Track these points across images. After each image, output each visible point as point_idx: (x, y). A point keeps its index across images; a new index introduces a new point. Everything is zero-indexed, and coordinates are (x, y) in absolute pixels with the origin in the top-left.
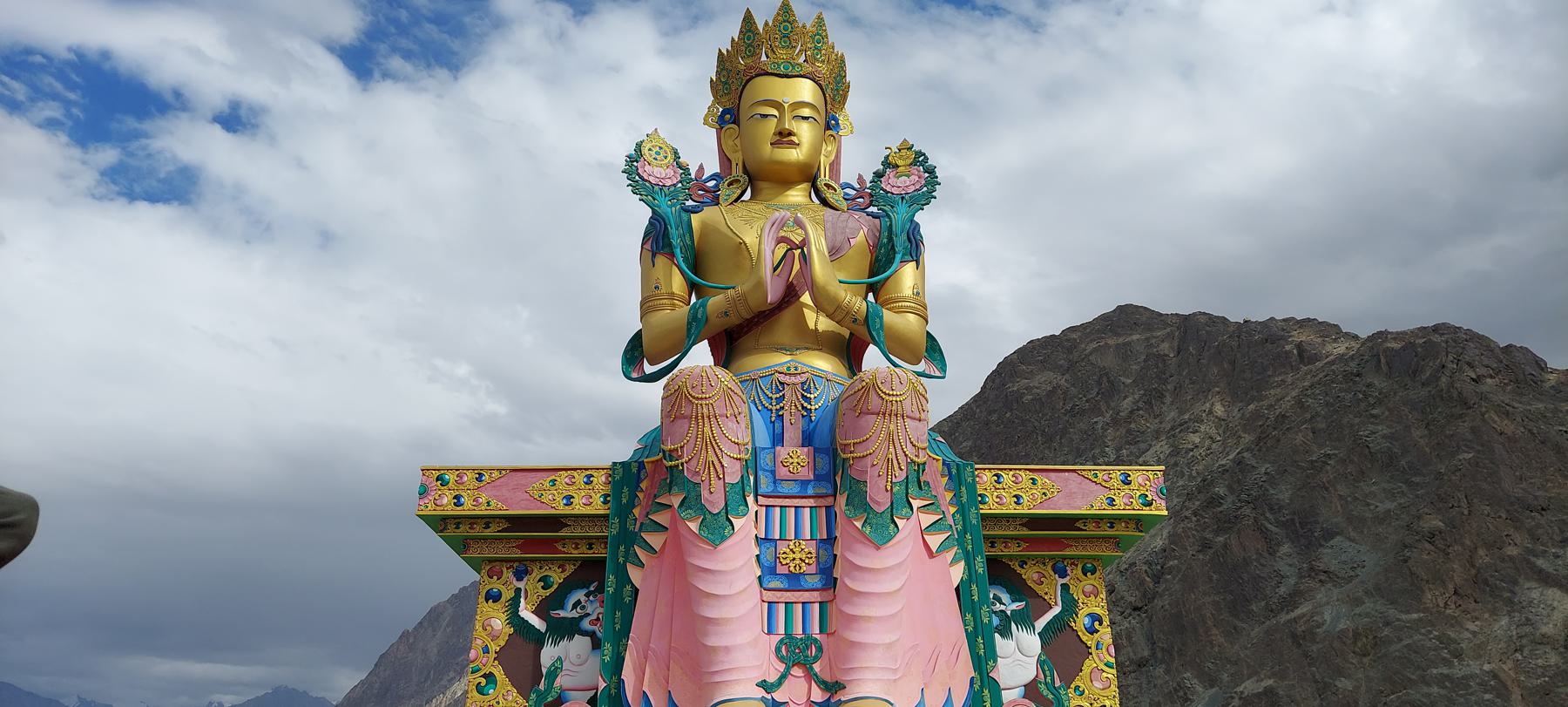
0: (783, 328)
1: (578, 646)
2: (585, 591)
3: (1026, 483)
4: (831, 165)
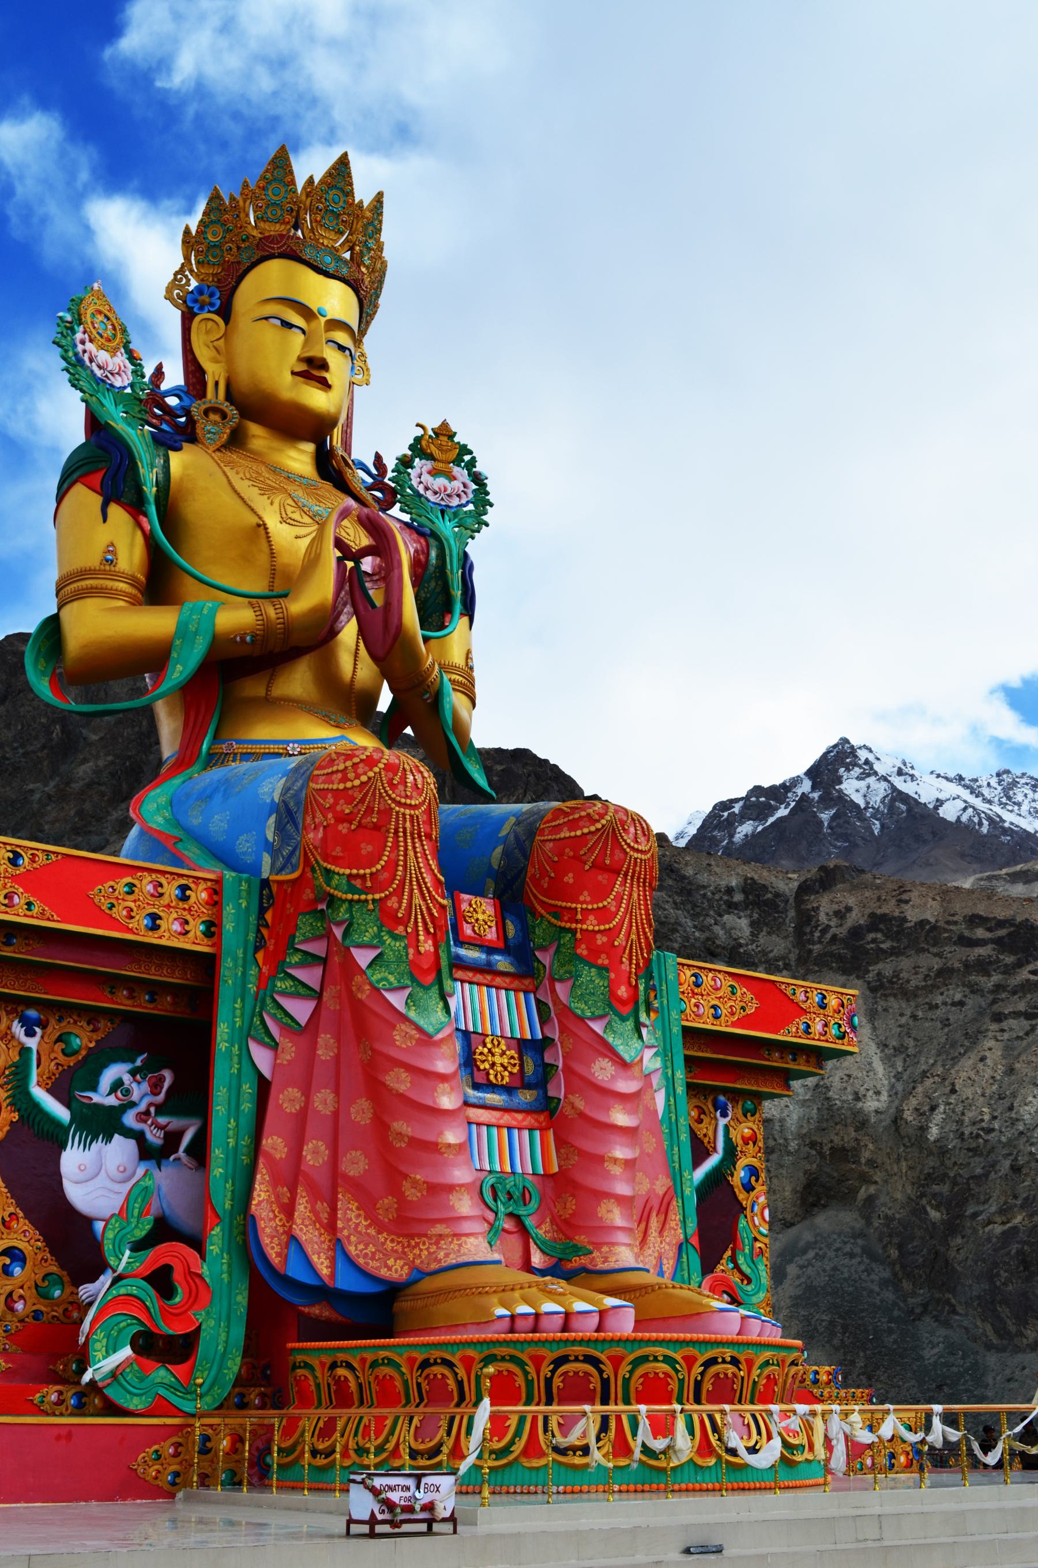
0: (298, 681)
1: (119, 1151)
2: (128, 1066)
3: (725, 990)
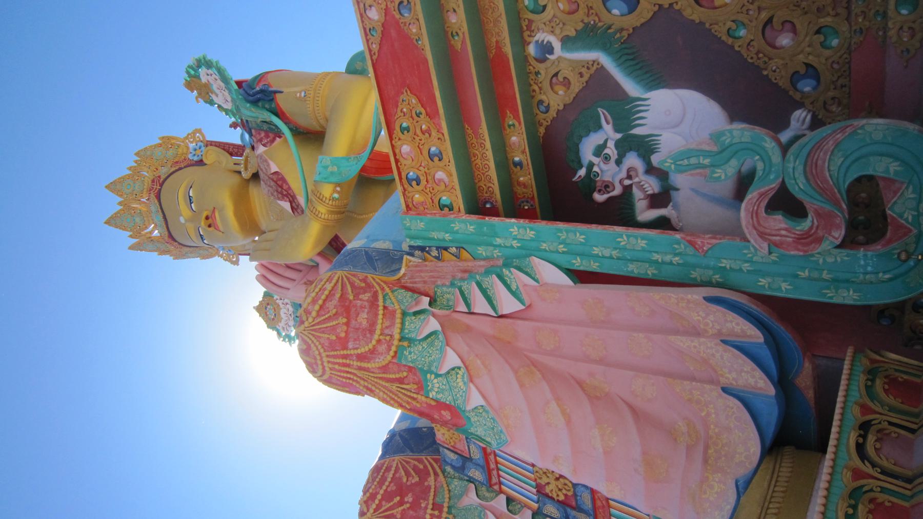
4: (231, 154)
